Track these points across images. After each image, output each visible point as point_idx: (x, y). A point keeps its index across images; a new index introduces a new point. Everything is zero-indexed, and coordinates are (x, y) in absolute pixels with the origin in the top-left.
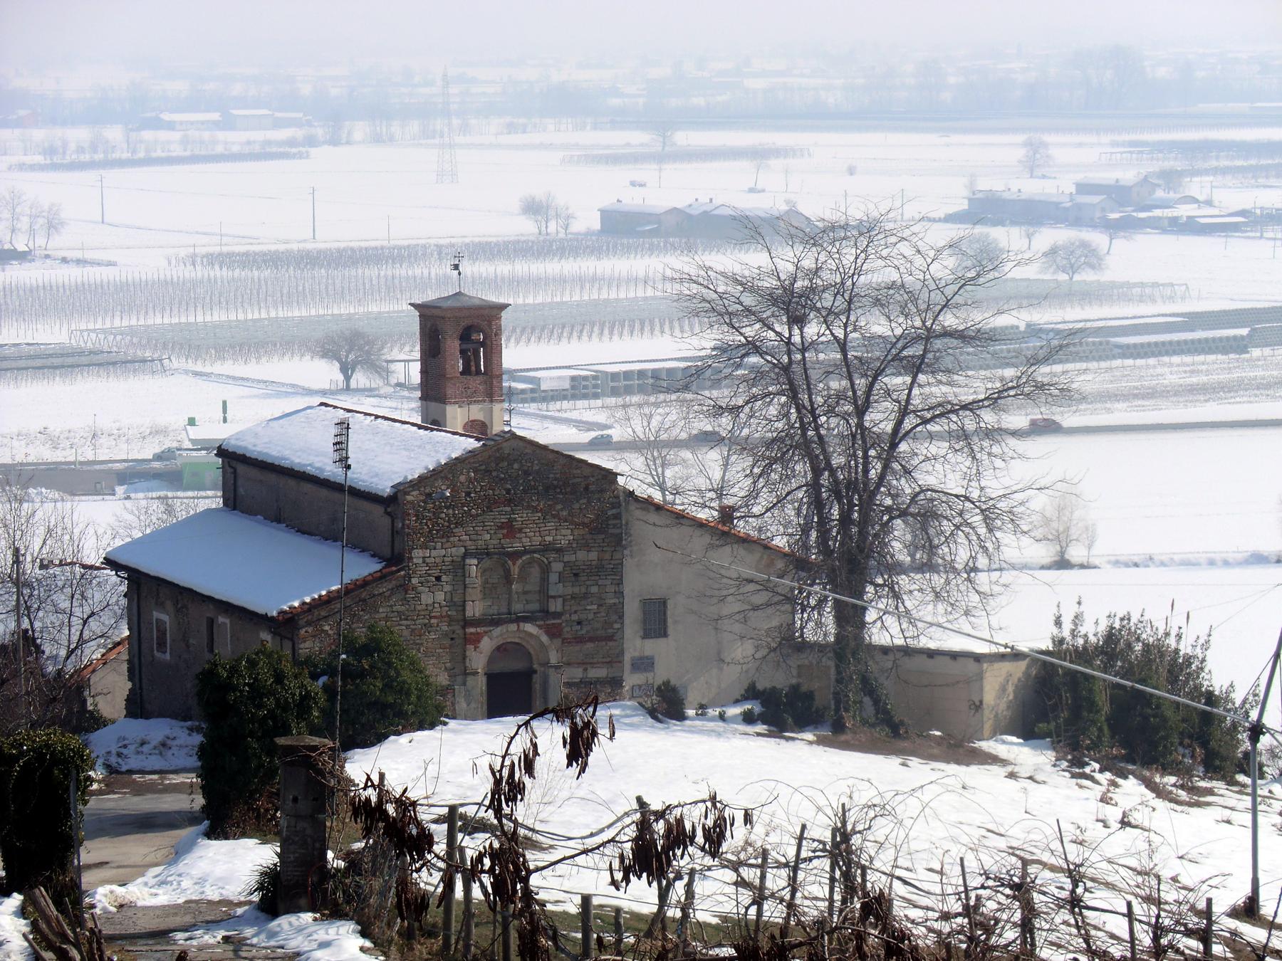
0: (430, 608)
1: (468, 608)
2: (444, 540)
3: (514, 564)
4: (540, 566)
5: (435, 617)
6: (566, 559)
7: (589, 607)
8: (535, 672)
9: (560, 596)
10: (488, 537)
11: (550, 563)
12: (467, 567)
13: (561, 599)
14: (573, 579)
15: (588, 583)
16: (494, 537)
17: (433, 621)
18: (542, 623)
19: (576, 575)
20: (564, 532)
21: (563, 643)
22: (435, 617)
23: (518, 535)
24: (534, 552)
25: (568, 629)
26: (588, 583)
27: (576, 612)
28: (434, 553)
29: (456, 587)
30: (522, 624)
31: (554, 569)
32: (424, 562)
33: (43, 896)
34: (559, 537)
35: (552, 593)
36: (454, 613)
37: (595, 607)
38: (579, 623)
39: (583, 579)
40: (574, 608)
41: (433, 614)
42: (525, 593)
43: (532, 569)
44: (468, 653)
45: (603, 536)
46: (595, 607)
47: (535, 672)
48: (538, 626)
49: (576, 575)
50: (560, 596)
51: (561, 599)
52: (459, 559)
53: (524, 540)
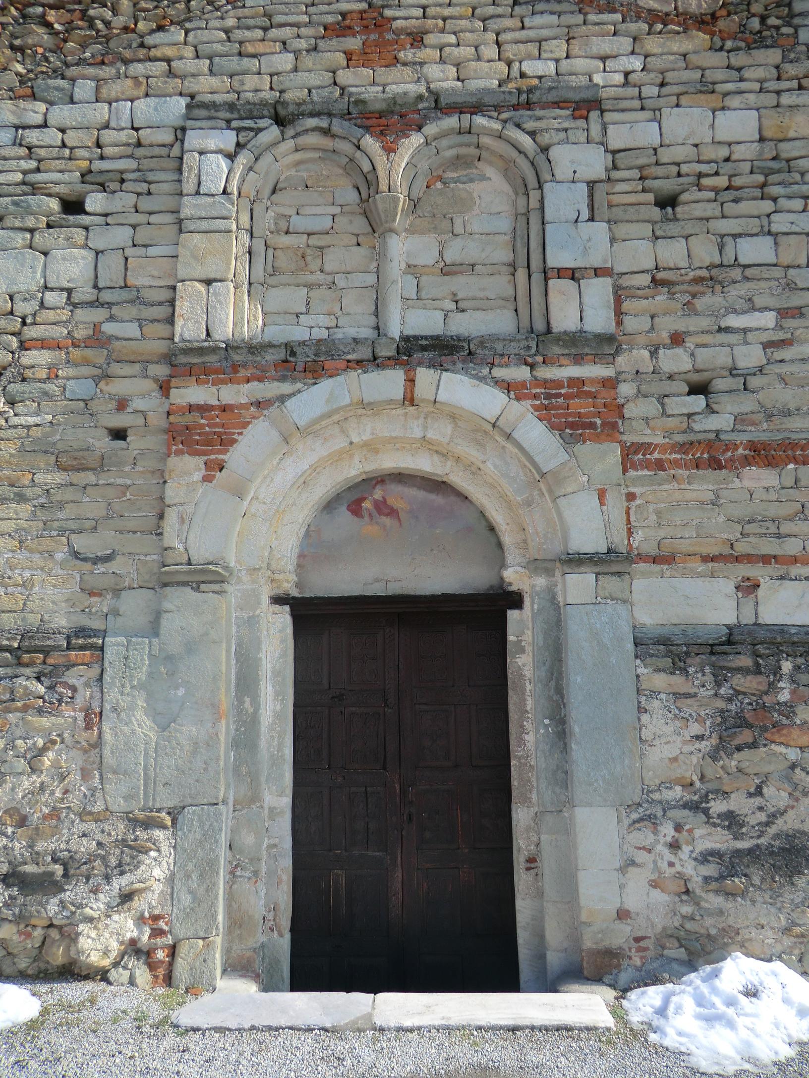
0: (23, 308)
1: (183, 307)
2: (107, 72)
3: (389, 150)
4: (507, 169)
5: (43, 344)
6: (618, 137)
7: (734, 321)
8: (515, 600)
9: (598, 272)
10: (285, 61)
11: (545, 150)
12: (191, 159)
13: (604, 285)
14: (656, 212)
15: (724, 226)
16: (308, 61)
17: (30, 357)
18: (522, 373)
19: (668, 202)
20: (605, 45)
21: (627, 463)
22: (43, 344)
23: (407, 55)
24: (476, 108)
25: (650, 407)
26: (724, 226)
27: (677, 339)
28: (61, 114)
29: (143, 235)
30: (425, 376)
31: (563, 170)
32: (17, 143)
33: (226, 826)
34: (580, 64)
35: (558, 258)
36: (132, 330)
37: (768, 319)
38: (699, 389)
39: (699, 210)
40: (668, 325)
41: (31, 332)
42: (447, 270)
43: (476, 188)
44: (171, 492)
45: (774, 56)
46: (768, 319)
47: (515, 600)
48: (508, 387)
49: (668, 202)
50: (598, 272)
51: (604, 285)
52: (167, 137)
53: (433, 71)
